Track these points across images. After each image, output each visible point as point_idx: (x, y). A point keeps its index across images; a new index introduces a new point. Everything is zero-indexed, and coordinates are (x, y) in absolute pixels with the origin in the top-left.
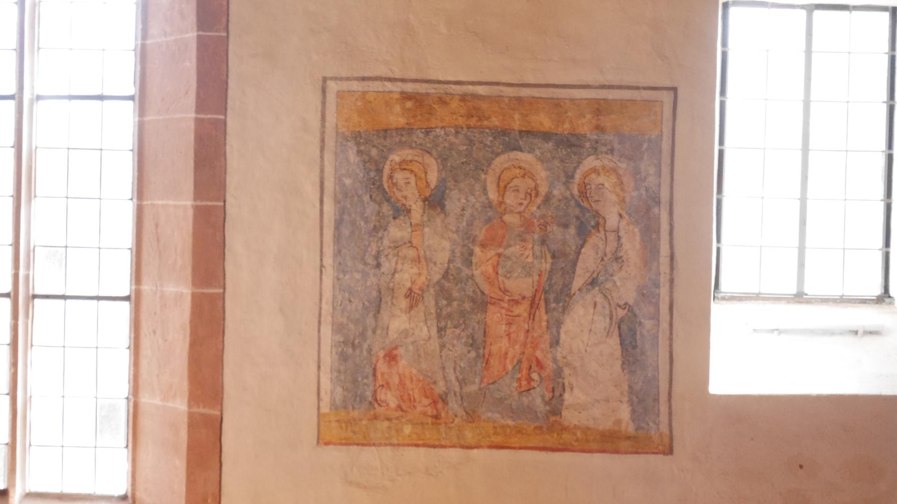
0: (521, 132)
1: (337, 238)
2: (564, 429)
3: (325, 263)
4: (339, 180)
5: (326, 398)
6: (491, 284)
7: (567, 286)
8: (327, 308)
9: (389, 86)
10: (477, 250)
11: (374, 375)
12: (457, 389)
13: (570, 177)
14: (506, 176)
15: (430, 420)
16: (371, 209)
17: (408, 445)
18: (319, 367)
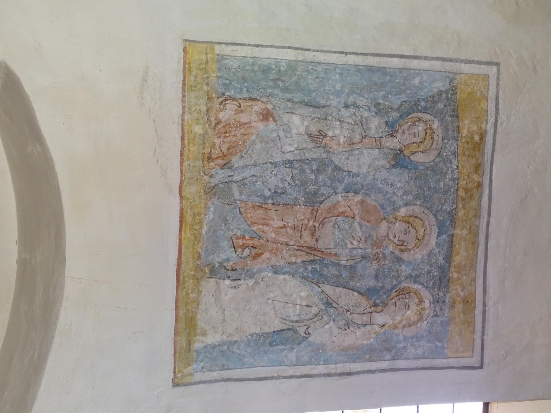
0: (453, 235)
1: (370, 69)
2: (198, 280)
3: (348, 56)
4: (418, 72)
5: (228, 50)
6: (329, 210)
7: (327, 280)
8: (310, 56)
9: (491, 120)
10: (359, 197)
11: (250, 99)
12: (236, 178)
13: (415, 279)
14: (417, 223)
15: (207, 151)
16: (395, 101)
17: (183, 130)
18: (257, 46)
